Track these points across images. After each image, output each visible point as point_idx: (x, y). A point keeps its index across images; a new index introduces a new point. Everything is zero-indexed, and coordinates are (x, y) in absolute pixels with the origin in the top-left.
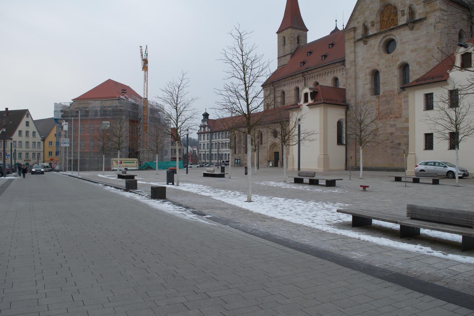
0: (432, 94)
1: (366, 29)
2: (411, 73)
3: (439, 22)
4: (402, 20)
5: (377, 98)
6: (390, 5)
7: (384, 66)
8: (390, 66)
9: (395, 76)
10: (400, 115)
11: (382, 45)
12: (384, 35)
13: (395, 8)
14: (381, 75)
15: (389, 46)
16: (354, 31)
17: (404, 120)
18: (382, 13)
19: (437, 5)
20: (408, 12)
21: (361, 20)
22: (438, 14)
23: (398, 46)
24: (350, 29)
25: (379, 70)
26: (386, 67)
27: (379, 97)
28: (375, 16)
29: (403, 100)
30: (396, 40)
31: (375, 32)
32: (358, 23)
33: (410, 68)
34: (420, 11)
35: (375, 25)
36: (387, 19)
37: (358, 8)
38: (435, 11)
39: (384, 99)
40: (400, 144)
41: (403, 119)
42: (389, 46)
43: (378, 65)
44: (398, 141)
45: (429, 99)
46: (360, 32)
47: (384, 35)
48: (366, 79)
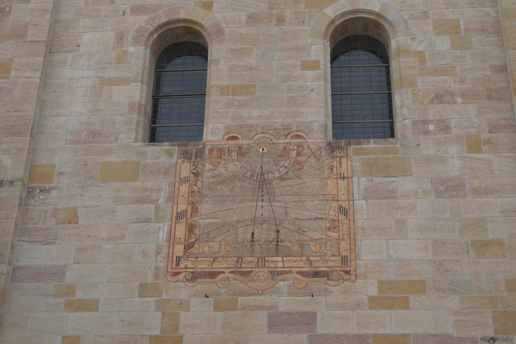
5: (186, 155)
7: (244, 17)
8: (280, 21)
9: (306, 66)
10: (344, 260)
17: (374, 291)
26: (253, 19)
27: (200, 154)
29: (360, 183)
48: (122, 58)
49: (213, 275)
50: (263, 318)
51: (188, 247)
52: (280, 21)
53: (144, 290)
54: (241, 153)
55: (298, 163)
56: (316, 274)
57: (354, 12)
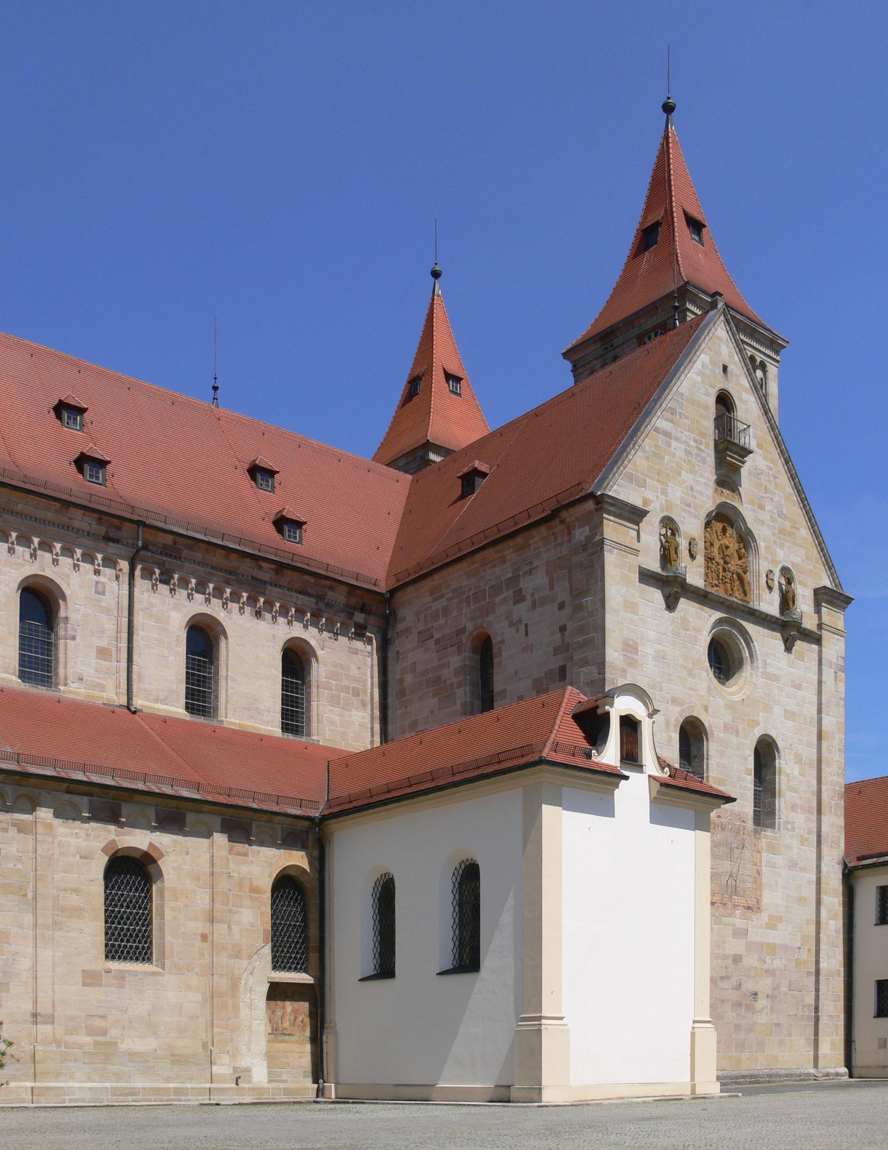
15: (724, 659)
40: (756, 994)
41: (764, 917)
44: (749, 986)
50: (730, 930)
55: (743, 839)
56: (749, 908)
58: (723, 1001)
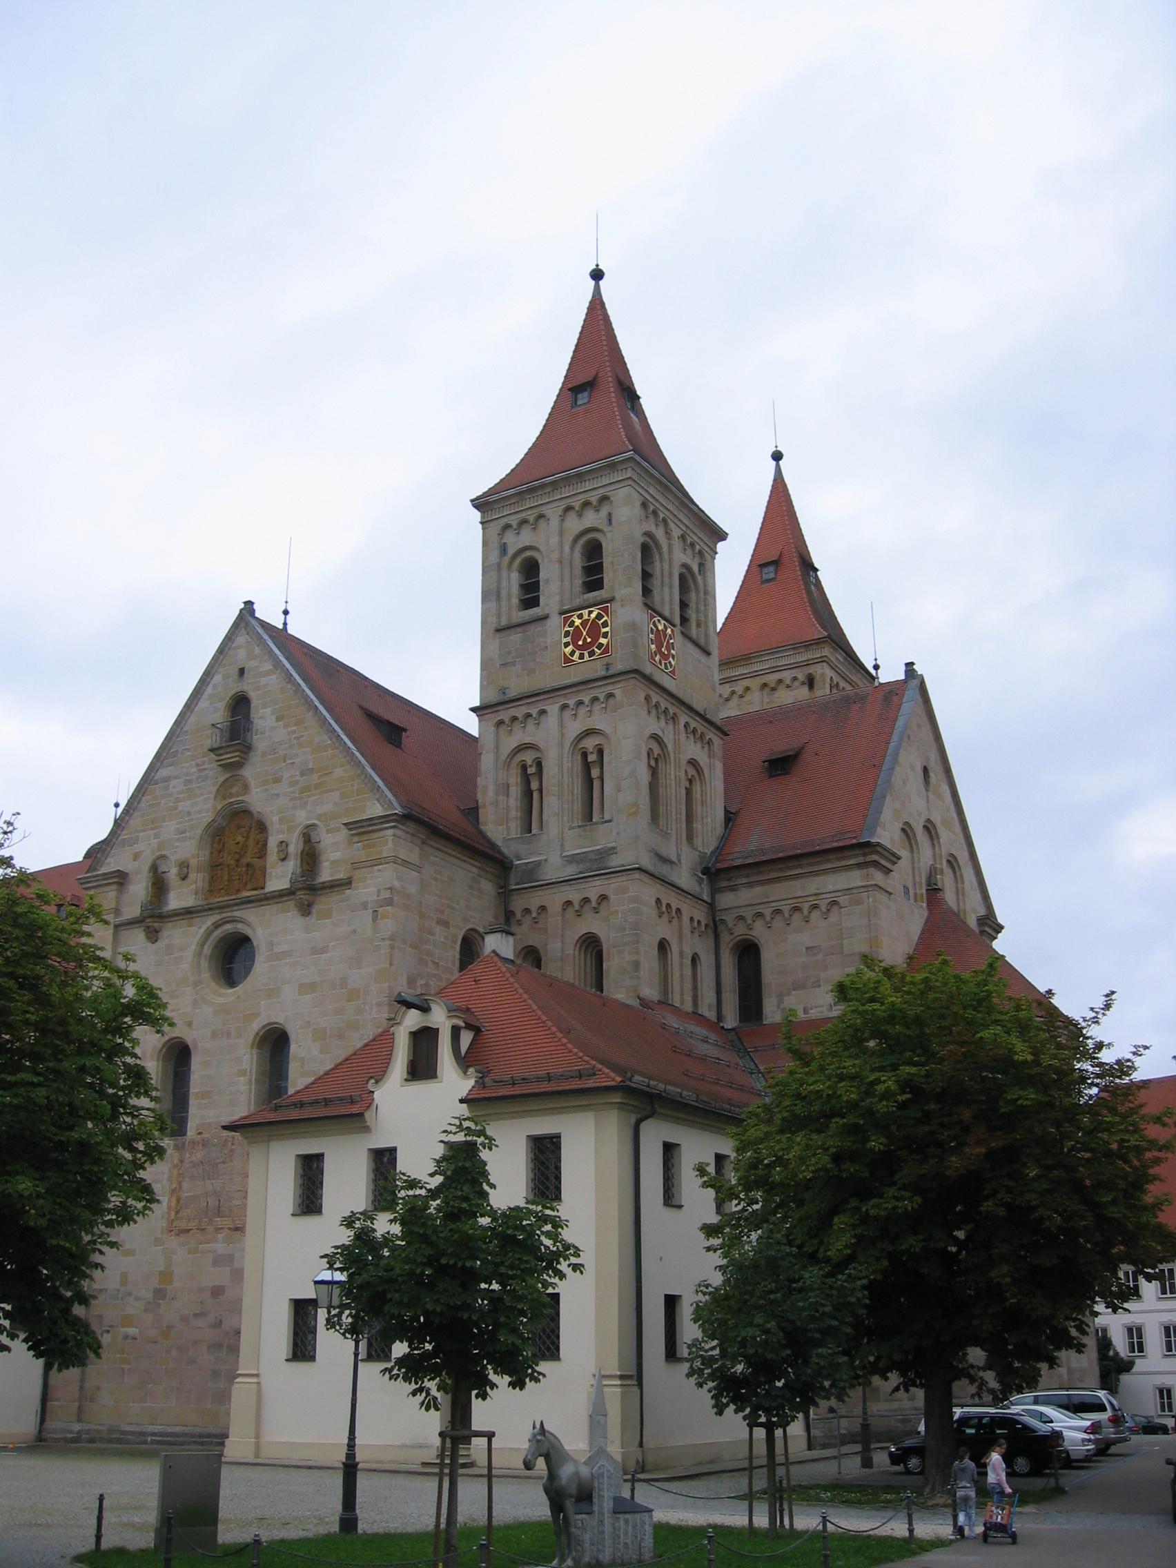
0: (319, 1157)
1: (159, 886)
2: (293, 1068)
3: (389, 902)
4: (279, 877)
6: (246, 812)
8: (228, 1035)
9: (242, 1073)
11: (207, 950)
12: (217, 917)
13: (262, 827)
14: (196, 1062)
16: (121, 884)
18: (217, 835)
19: (386, 843)
20: (301, 847)
21: (147, 848)
22: (387, 875)
23: (261, 966)
24: (106, 876)
25: (189, 1042)
26: (214, 1035)
27: (184, 1144)
28: (194, 842)
30: (255, 944)
31: (189, 901)
32: (136, 856)
33: (293, 1048)
34: (336, 856)
35: (192, 876)
36: (233, 862)
37: (143, 805)
38: (379, 862)
39: (199, 1155)
42: (232, 957)
43: (190, 1024)
45: (311, 1172)
46: (139, 890)
47: (218, 917)
49: (188, 1231)
51: (177, 1213)
52: (228, 1035)
53: (158, 1242)
54: (205, 1144)
57: (270, 1024)
58: (196, 1342)
